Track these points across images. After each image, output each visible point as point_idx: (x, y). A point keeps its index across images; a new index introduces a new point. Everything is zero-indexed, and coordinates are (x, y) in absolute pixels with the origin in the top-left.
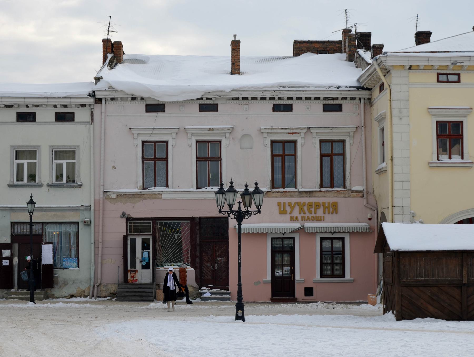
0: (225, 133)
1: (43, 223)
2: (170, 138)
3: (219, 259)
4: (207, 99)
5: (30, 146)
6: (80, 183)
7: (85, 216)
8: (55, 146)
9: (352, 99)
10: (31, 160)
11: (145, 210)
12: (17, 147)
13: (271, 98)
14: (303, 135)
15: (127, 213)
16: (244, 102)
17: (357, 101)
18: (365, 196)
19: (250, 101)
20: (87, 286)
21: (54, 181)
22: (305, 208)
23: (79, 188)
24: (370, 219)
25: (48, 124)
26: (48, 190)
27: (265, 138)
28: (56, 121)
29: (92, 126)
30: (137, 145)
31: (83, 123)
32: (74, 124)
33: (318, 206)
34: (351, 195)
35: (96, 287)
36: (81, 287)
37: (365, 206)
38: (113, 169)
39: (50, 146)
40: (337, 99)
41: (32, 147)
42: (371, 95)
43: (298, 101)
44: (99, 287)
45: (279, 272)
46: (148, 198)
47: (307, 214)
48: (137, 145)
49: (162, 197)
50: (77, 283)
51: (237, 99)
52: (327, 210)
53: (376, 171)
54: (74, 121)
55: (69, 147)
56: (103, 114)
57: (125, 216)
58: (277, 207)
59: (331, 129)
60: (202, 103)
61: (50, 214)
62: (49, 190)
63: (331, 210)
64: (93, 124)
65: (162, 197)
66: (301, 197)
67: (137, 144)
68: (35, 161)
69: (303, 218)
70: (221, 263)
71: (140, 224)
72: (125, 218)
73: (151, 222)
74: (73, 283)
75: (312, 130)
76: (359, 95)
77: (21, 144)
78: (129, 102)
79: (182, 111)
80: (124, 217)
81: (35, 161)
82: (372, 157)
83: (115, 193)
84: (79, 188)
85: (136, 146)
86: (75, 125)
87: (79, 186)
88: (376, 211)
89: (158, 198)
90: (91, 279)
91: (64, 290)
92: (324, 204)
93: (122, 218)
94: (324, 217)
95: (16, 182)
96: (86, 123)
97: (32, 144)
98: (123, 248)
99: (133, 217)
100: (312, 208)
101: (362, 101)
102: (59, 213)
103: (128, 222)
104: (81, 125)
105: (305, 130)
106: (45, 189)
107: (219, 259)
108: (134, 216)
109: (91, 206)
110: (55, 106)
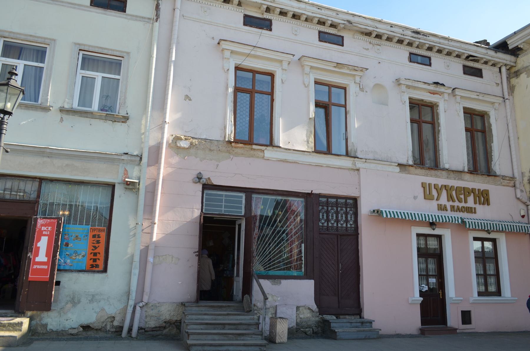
0: (354, 76)
1: (41, 180)
2: (278, 69)
4: (332, 26)
5: (35, 37)
6: (123, 113)
8: (84, 45)
11: (236, 174)
12: (6, 34)
13: (410, 44)
14: (446, 96)
16: (376, 42)
18: (518, 185)
19: (383, 42)
20: (120, 306)
21: (75, 106)
23: (122, 122)
24: (523, 217)
25: (76, 7)
26: (60, 118)
27: (403, 92)
28: (91, 5)
29: (157, 24)
30: (228, 70)
31: (141, 19)
32: (125, 16)
33: (467, 192)
34: (502, 183)
35: (138, 308)
36: (106, 308)
37: (518, 199)
38: (186, 100)
39: (76, 44)
41: (39, 40)
42: (515, 63)
43: (438, 55)
44: (145, 309)
45: (424, 287)
46: (242, 154)
47: (456, 204)
48: (228, 70)
49: (265, 156)
50: (100, 301)
51: (369, 34)
52: (478, 198)
54: (124, 11)
55: (110, 53)
56: (177, 12)
57: (201, 181)
58: (422, 189)
59: (478, 95)
60: (323, 30)
61: (57, 162)
62: (62, 120)
63: (482, 199)
64: (158, 21)
65: (264, 156)
66: (448, 179)
67: (228, 68)
68: (41, 65)
69: (452, 207)
71: (224, 198)
72: (201, 184)
73: (243, 195)
74: (91, 301)
75: (457, 92)
76: (504, 59)
77: (16, 30)
78: (220, 6)
79: (296, 35)
80: (199, 182)
81: (41, 65)
82: (518, 138)
84: (123, 124)
85: (226, 71)
86: (126, 18)
89: (258, 157)
90: (128, 293)
91: (69, 315)
92: (473, 191)
94: (475, 208)
96: (147, 20)
97: (41, 33)
99: (215, 183)
100: (461, 195)
101: (504, 69)
102: (78, 164)
103: (205, 192)
104: (136, 20)
106: (54, 115)
109: (141, 155)
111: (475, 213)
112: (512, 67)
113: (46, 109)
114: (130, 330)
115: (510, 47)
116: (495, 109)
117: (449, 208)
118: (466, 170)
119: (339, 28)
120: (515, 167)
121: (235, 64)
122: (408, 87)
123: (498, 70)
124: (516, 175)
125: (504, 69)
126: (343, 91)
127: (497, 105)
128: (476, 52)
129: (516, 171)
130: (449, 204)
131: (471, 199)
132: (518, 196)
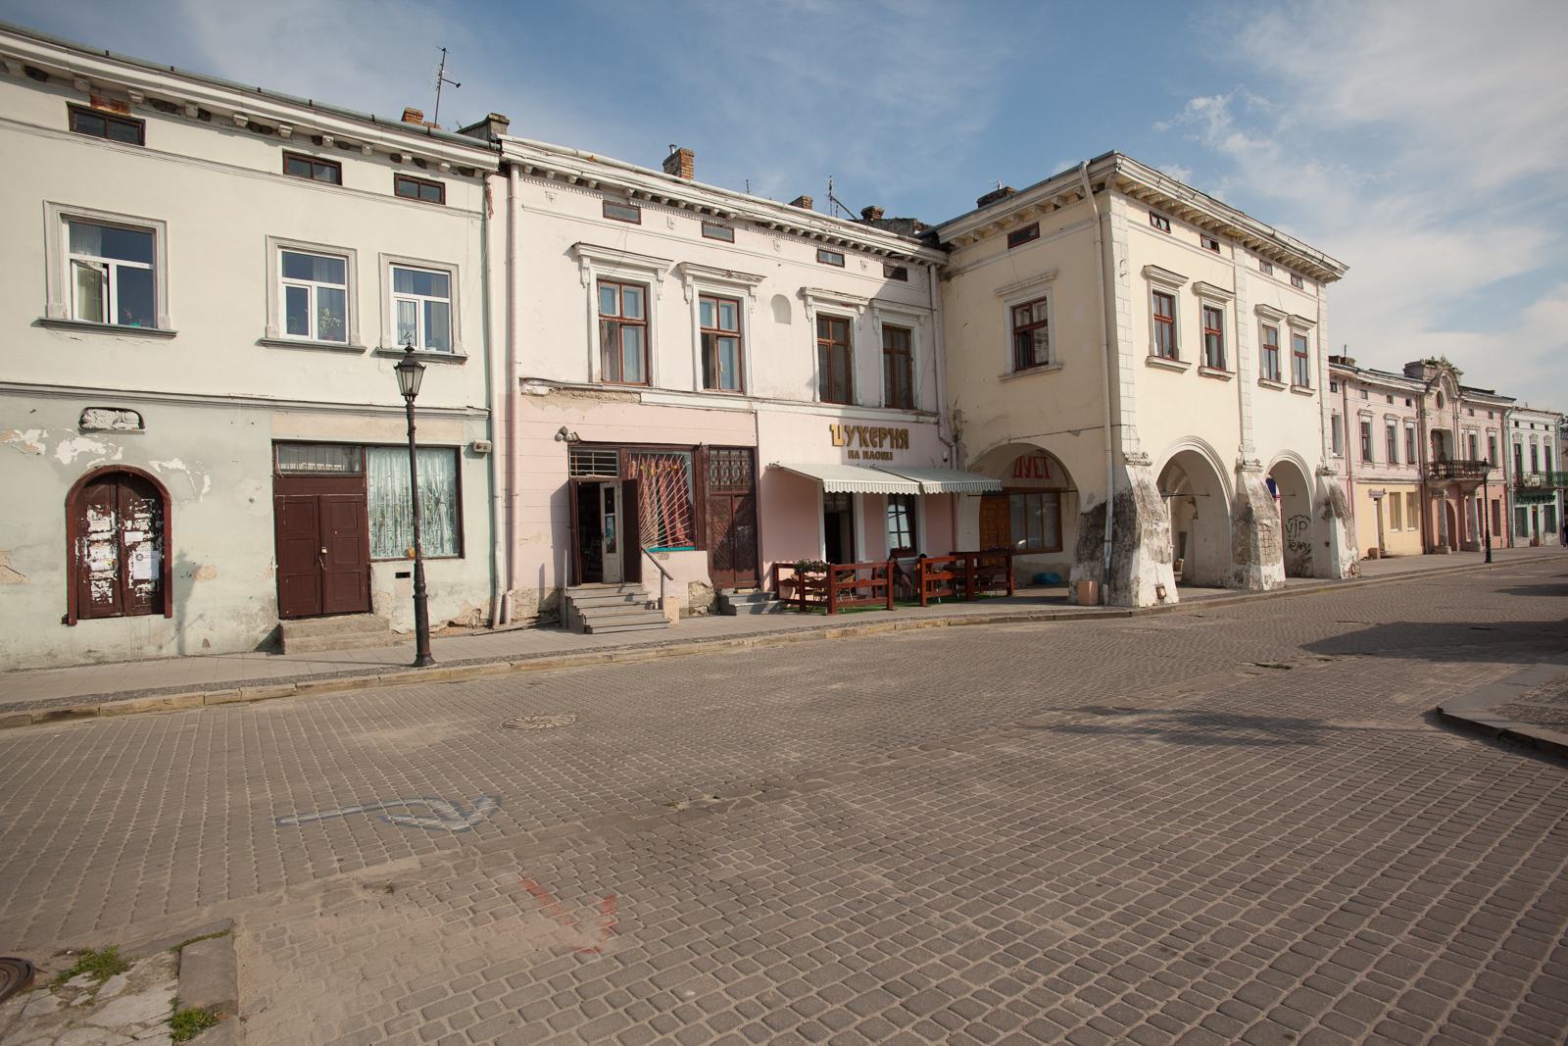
3: (739, 529)
7: (477, 433)
9: (922, 263)
10: (330, 282)
15: (570, 431)
17: (924, 269)
22: (868, 436)
24: (946, 460)
25: (378, 197)
32: (446, 210)
37: (941, 439)
40: (902, 258)
42: (947, 261)
47: (870, 449)
53: (1000, 377)
58: (830, 433)
69: (865, 454)
70: (744, 536)
74: (451, 593)
76: (933, 257)
83: (545, 383)
87: (460, 361)
88: (954, 449)
92: (890, 431)
93: (557, 439)
95: (284, 335)
98: (549, 508)
101: (933, 269)
104: (462, 216)
105: (866, 303)
107: (739, 529)
108: (586, 436)
110: (396, 158)
111: (891, 459)
112: (942, 266)
113: (360, 351)
114: (502, 622)
115: (941, 242)
116: (920, 324)
117: (861, 454)
118: (883, 403)
119: (728, 218)
120: (940, 400)
121: (598, 275)
122: (816, 299)
123: (926, 270)
124: (941, 410)
125: (933, 269)
126: (735, 304)
127: (922, 319)
128: (900, 247)
129: (940, 404)
130: (861, 451)
131: (887, 442)
132: (941, 435)
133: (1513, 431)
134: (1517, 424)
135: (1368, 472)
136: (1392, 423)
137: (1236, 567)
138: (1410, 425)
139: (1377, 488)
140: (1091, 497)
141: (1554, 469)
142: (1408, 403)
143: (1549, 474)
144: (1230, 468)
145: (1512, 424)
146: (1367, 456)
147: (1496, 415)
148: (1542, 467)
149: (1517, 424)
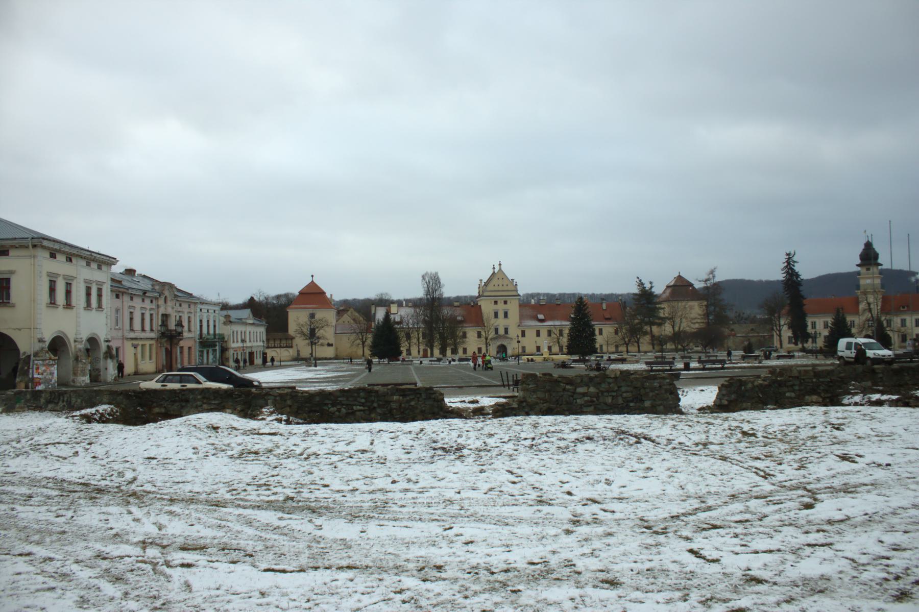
133: (198, 314)
134: (201, 310)
135: (132, 335)
136: (144, 312)
137: (72, 377)
138: (152, 312)
139: (135, 342)
140: (24, 353)
141: (217, 332)
142: (152, 302)
143: (215, 334)
144: (72, 341)
145: (199, 310)
146: (132, 330)
147: (192, 306)
148: (212, 331)
149: (201, 310)
